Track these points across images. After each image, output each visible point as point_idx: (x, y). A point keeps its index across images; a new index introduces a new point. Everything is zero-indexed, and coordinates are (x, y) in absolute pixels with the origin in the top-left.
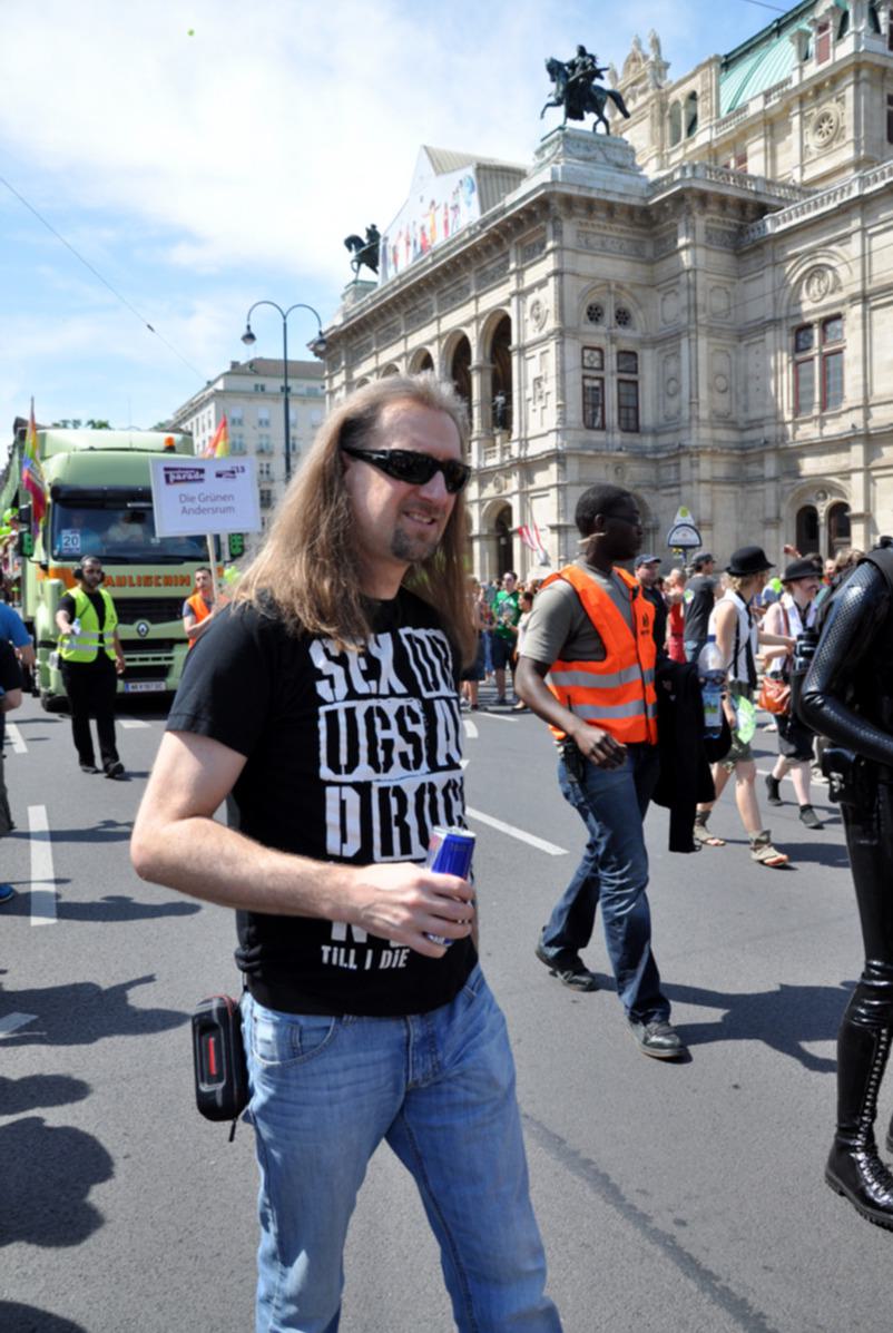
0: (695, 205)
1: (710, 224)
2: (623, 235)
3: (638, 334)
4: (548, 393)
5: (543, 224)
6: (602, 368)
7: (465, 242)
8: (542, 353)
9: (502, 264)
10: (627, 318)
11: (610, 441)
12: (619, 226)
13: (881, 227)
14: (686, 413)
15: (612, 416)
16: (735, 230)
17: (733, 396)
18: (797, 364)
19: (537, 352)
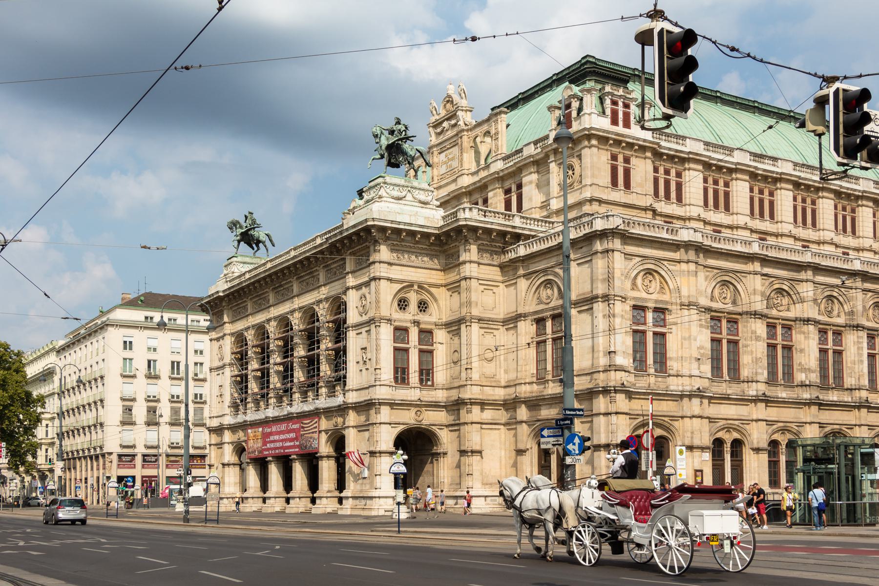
0: (470, 235)
1: (481, 247)
2: (422, 252)
3: (434, 319)
4: (370, 359)
5: (367, 244)
6: (408, 343)
7: (315, 247)
8: (366, 331)
9: (342, 265)
10: (426, 308)
11: (413, 394)
12: (420, 246)
13: (583, 260)
14: (463, 375)
15: (414, 377)
16: (500, 250)
17: (498, 363)
18: (538, 343)
19: (364, 330)
